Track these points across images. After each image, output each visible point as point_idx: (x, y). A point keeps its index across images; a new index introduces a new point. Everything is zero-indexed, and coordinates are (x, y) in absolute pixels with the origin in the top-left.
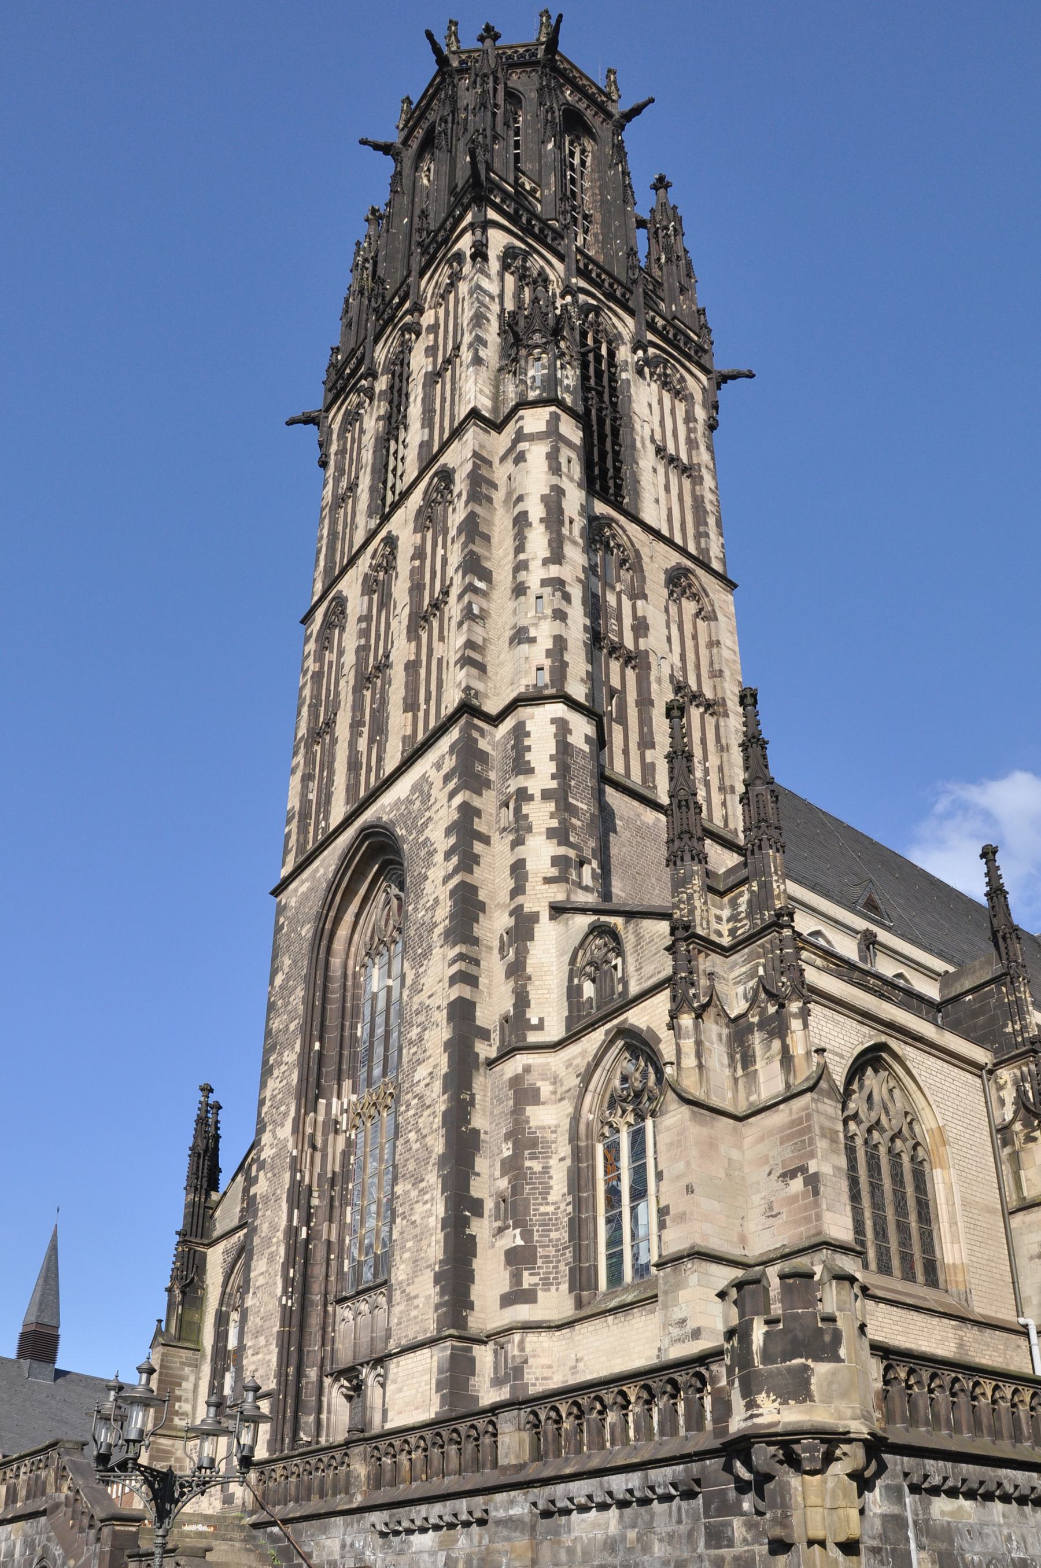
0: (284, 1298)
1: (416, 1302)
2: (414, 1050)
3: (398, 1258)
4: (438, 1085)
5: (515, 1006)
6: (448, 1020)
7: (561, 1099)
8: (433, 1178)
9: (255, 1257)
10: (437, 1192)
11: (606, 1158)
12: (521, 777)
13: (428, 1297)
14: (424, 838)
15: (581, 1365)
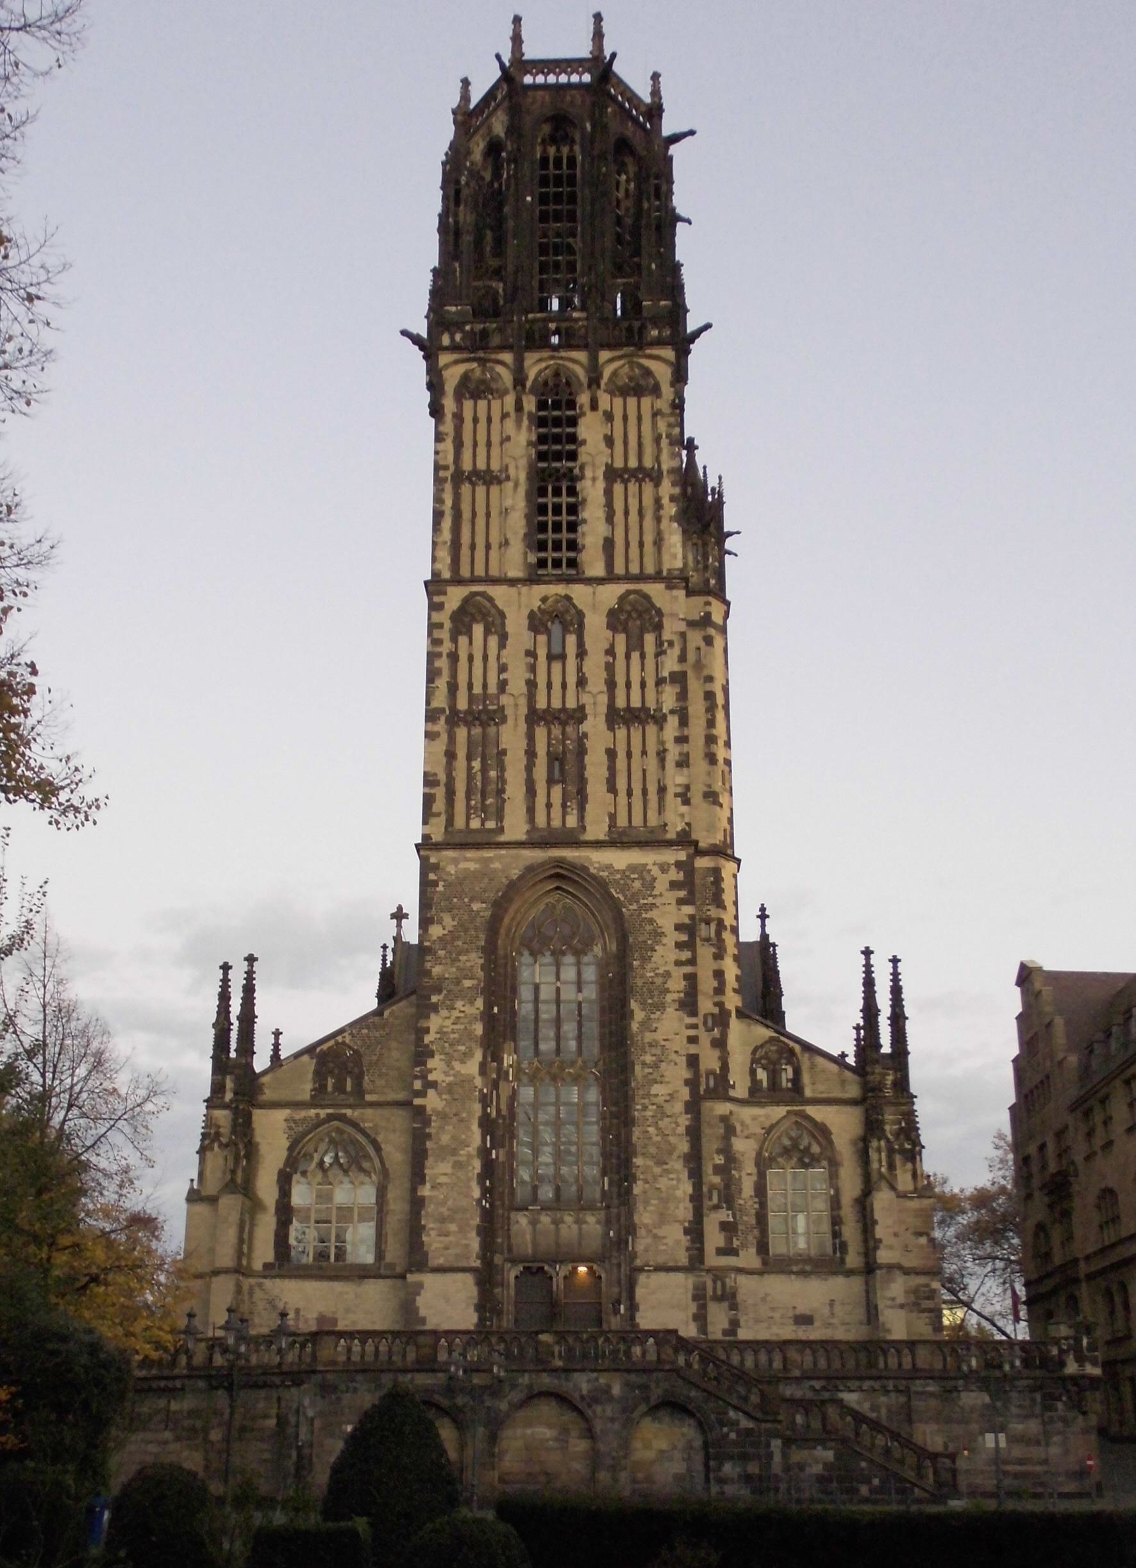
1: (665, 1241)
2: (647, 1070)
4: (679, 1107)
5: (721, 1069)
7: (747, 1137)
8: (678, 1165)
10: (685, 1175)
12: (720, 910)
13: (678, 1242)
14: (648, 916)
15: (769, 1298)
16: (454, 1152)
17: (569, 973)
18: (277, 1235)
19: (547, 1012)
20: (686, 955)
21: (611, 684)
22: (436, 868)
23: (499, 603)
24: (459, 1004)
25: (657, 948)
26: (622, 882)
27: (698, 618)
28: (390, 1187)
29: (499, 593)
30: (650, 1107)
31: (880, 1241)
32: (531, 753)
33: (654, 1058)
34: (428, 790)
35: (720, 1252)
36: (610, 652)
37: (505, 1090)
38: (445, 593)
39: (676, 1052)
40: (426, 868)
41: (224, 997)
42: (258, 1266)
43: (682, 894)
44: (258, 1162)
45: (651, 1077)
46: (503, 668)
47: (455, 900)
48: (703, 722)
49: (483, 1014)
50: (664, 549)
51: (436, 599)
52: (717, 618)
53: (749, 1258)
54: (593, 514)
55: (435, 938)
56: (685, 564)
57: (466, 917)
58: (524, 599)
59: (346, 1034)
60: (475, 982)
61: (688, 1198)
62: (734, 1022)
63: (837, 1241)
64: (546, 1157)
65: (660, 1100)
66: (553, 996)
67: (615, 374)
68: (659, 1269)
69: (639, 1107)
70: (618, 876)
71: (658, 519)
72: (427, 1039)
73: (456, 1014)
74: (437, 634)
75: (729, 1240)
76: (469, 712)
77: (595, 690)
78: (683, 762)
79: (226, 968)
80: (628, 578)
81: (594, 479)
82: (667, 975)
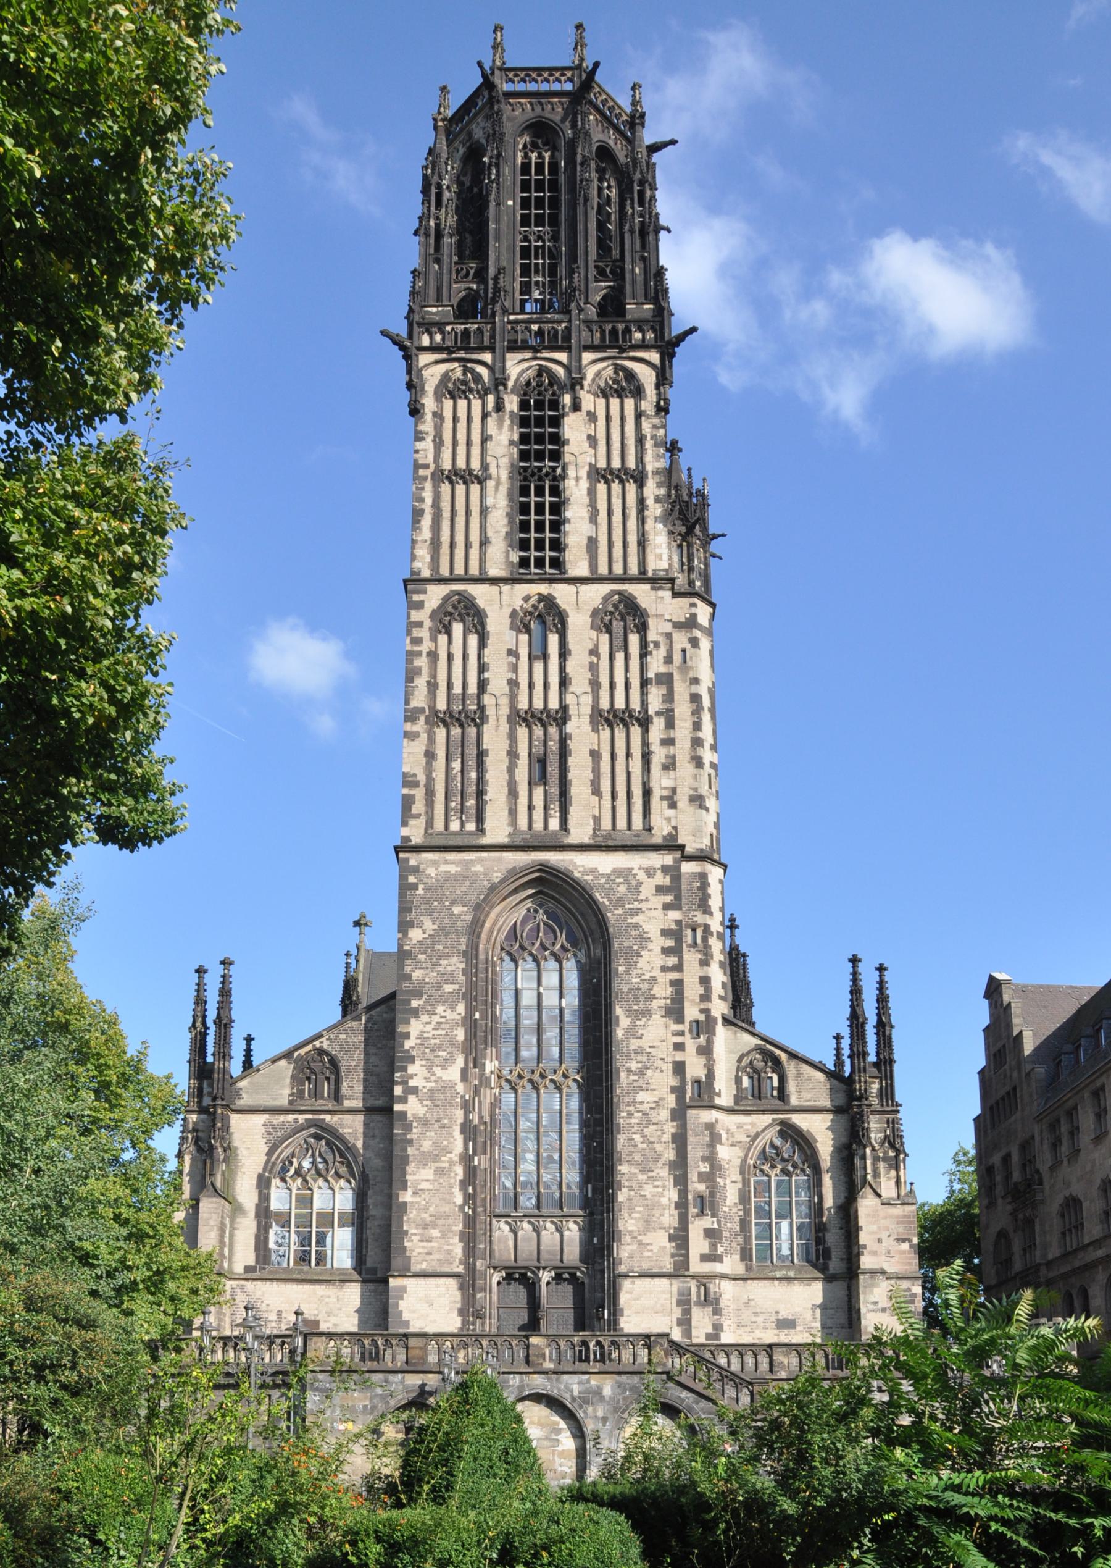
0: (466, 1208)
1: (649, 1247)
2: (632, 1077)
3: (626, 1215)
4: (664, 1114)
5: (706, 1076)
6: (674, 1073)
7: (732, 1145)
8: (664, 1172)
9: (412, 1165)
10: (670, 1182)
11: (755, 1188)
15: (752, 1303)
16: (436, 1158)
17: (551, 978)
18: (257, 1237)
19: (528, 1020)
20: (672, 961)
21: (595, 684)
22: (416, 870)
23: (481, 603)
24: (440, 1009)
25: (642, 953)
26: (607, 886)
27: (683, 620)
28: (370, 1192)
29: (481, 594)
30: (636, 1115)
31: (865, 1247)
32: (513, 754)
33: (640, 1065)
34: (405, 791)
35: (705, 1258)
36: (594, 652)
37: (487, 1097)
38: (425, 592)
39: (662, 1059)
40: (405, 870)
41: (200, 1001)
42: (239, 1269)
43: (669, 899)
44: (237, 1167)
45: (635, 1084)
46: (482, 668)
47: (436, 903)
48: (689, 725)
49: (464, 1019)
50: (648, 550)
51: (416, 598)
52: (703, 617)
53: (731, 1264)
54: (576, 513)
55: (414, 942)
56: (670, 565)
57: (446, 921)
58: (504, 597)
59: (323, 1039)
60: (456, 987)
61: (673, 1206)
62: (720, 1030)
63: (821, 1247)
64: (528, 1164)
65: (645, 1107)
66: (535, 1002)
67: (598, 374)
68: (642, 1275)
69: (623, 1114)
70: (603, 881)
71: (642, 520)
72: (408, 1044)
73: (436, 1019)
74: (416, 632)
75: (713, 1246)
76: (449, 711)
77: (579, 691)
78: (670, 765)
79: (201, 971)
80: (611, 578)
81: (577, 479)
82: (653, 980)
